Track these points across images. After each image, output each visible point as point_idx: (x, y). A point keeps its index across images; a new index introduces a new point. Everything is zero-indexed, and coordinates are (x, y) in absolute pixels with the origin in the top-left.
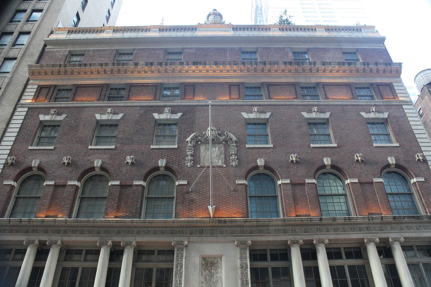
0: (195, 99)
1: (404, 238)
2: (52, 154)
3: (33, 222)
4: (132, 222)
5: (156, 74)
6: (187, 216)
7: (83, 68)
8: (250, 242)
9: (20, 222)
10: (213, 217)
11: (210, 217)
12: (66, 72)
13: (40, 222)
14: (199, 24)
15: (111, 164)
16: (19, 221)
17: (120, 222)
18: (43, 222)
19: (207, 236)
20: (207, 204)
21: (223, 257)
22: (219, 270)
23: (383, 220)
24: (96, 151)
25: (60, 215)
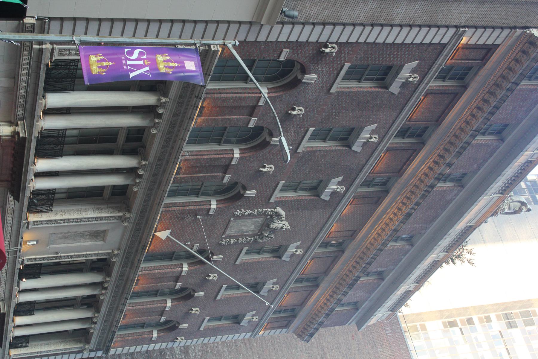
0: (348, 206)
1: (93, 333)
2: (319, 92)
3: (193, 109)
4: (163, 191)
5: (419, 174)
6: (162, 217)
7: (487, 109)
8: (114, 260)
9: (198, 97)
10: (154, 235)
11: (155, 232)
12: (497, 85)
13: (191, 115)
14: (485, 222)
15: (269, 153)
16: (200, 96)
17: (167, 182)
18: (190, 119)
19: (128, 240)
20: (174, 229)
21: (102, 242)
22: (88, 240)
23: (114, 327)
24: (300, 136)
25: (200, 120)
